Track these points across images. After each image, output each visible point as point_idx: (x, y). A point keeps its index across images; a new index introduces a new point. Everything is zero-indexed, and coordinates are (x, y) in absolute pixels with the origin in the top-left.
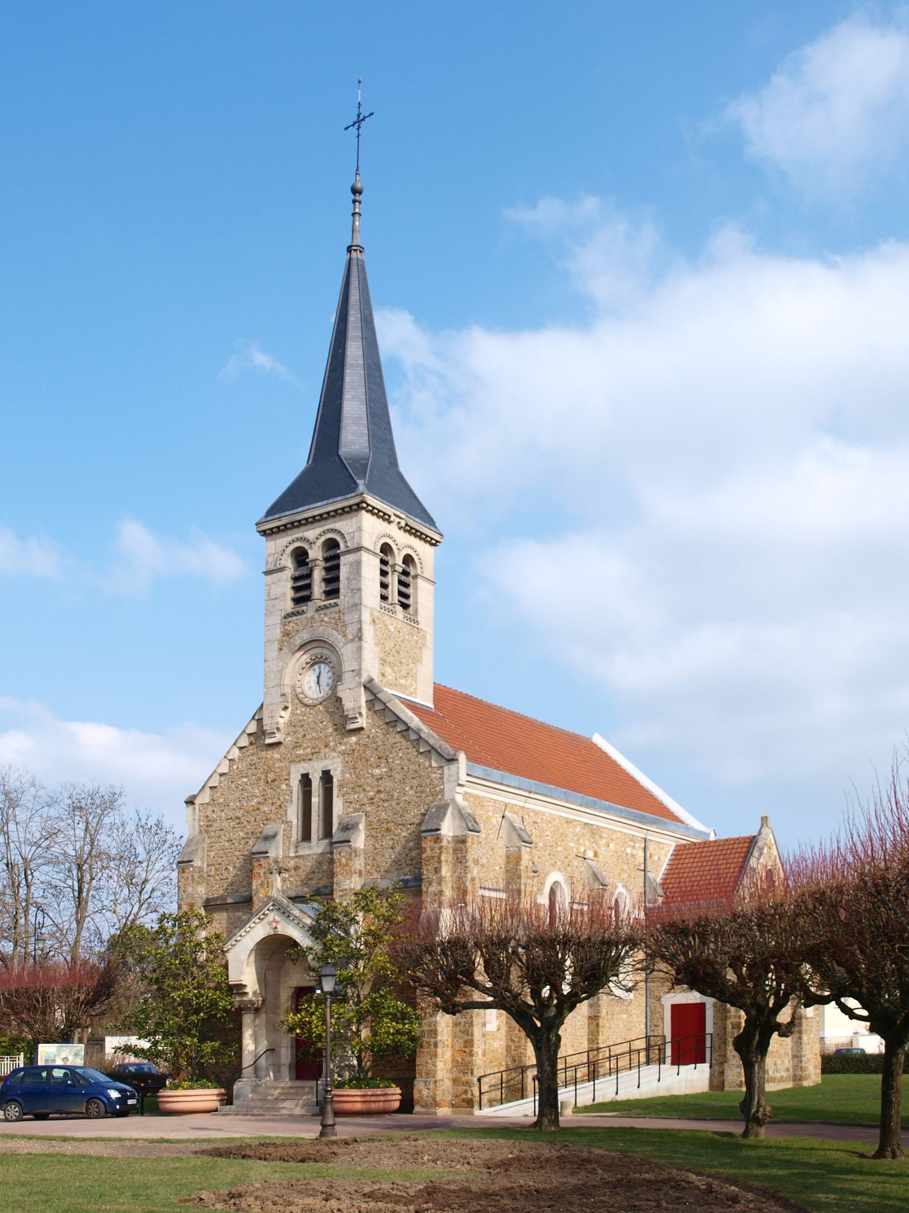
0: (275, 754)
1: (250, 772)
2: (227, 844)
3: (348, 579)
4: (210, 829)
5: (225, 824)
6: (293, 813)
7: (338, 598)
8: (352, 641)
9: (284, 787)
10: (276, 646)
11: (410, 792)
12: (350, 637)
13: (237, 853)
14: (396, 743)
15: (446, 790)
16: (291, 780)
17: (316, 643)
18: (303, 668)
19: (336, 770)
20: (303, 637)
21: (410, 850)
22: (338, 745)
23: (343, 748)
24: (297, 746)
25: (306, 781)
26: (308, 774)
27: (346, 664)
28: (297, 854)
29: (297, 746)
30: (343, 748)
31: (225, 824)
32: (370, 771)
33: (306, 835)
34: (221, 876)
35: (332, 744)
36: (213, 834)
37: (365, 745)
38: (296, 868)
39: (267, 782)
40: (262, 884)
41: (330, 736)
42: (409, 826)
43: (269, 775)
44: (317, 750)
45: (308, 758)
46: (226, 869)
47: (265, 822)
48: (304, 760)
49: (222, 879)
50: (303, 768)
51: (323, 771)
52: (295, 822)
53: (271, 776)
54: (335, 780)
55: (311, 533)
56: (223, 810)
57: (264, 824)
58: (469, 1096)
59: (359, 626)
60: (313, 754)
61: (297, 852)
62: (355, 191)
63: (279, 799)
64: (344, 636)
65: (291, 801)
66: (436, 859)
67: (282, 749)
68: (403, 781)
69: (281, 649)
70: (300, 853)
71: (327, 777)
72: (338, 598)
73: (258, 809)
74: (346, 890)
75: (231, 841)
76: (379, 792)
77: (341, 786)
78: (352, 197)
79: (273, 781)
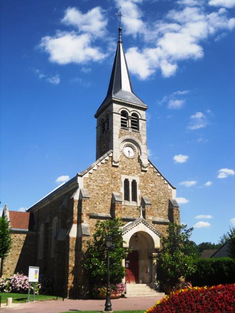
0: (116, 169)
1: (105, 172)
3: (142, 127)
5: (95, 187)
6: (122, 190)
21: (163, 211)
25: (126, 181)
31: (95, 187)
35: (136, 172)
38: (124, 209)
40: (119, 212)
46: (96, 203)
53: (114, 176)
54: (137, 184)
55: (131, 109)
67: (118, 168)
68: (159, 190)
70: (126, 204)
71: (134, 182)
76: (152, 191)
77: (140, 186)
79: (115, 178)
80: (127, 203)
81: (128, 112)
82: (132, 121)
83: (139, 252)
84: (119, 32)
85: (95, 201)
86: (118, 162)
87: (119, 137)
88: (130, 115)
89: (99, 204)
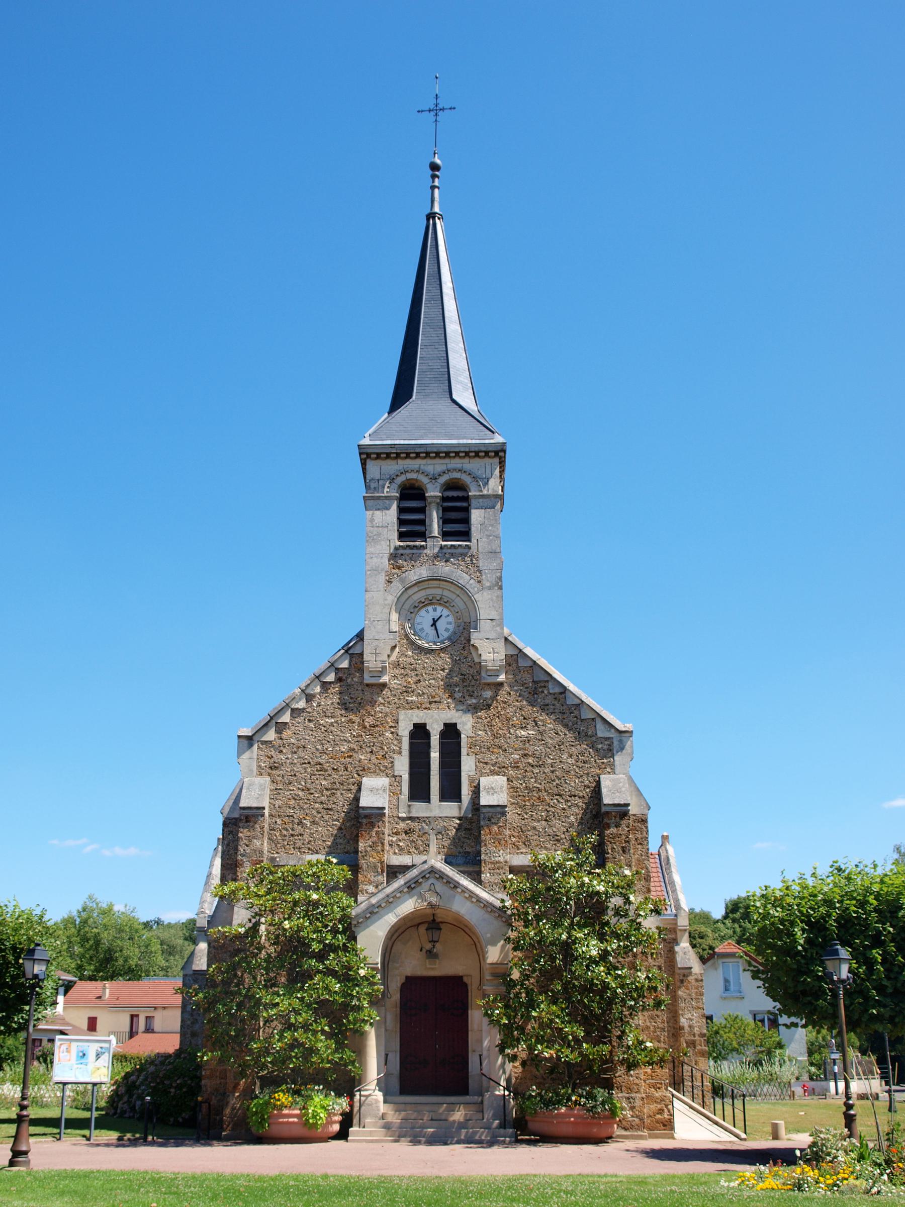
2: (300, 793)
4: (274, 772)
6: (402, 766)
7: (470, 541)
8: (490, 588)
9: (388, 734)
10: (382, 578)
11: (569, 760)
12: (488, 584)
13: (317, 805)
14: (547, 705)
15: (617, 763)
16: (400, 729)
17: (438, 582)
18: (415, 607)
19: (464, 724)
20: (421, 574)
22: (467, 697)
23: (474, 701)
24: (407, 690)
25: (420, 732)
26: (424, 725)
27: (482, 611)
28: (412, 815)
29: (407, 690)
30: (474, 701)
32: (512, 731)
33: (419, 792)
34: (291, 832)
36: (279, 779)
37: (505, 703)
39: (365, 727)
41: (456, 686)
42: (569, 799)
43: (367, 720)
44: (437, 699)
45: (424, 706)
46: (300, 823)
47: (361, 773)
48: (418, 708)
49: (292, 835)
50: (418, 716)
51: (414, 724)
52: (406, 777)
54: (463, 736)
56: (295, 753)
57: (359, 775)
58: (666, 1116)
59: (499, 574)
60: (430, 703)
61: (409, 812)
62: (434, 167)
63: (382, 748)
64: (479, 582)
65: (400, 753)
66: (624, 837)
69: (390, 582)
70: (414, 814)
71: (451, 732)
72: (470, 541)
73: (350, 757)
74: (499, 862)
75: (308, 790)
76: (525, 755)
78: (431, 172)
80: (420, 809)
81: (424, 480)
82: (445, 510)
83: (465, 979)
84: (434, 177)
85: (299, 814)
86: (384, 668)
87: (390, 582)
88: (433, 492)
89: (314, 823)
